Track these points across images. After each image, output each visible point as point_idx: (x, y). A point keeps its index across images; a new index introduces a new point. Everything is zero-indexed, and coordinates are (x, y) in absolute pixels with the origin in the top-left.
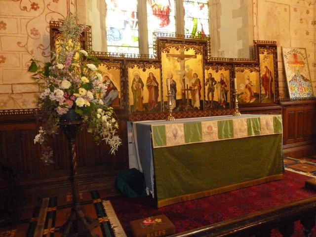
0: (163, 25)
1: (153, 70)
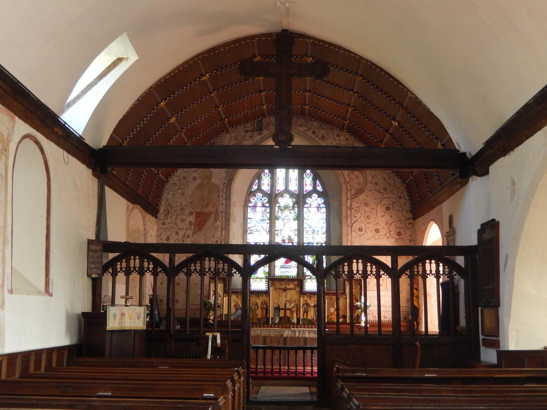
0: (287, 262)
1: (264, 298)
